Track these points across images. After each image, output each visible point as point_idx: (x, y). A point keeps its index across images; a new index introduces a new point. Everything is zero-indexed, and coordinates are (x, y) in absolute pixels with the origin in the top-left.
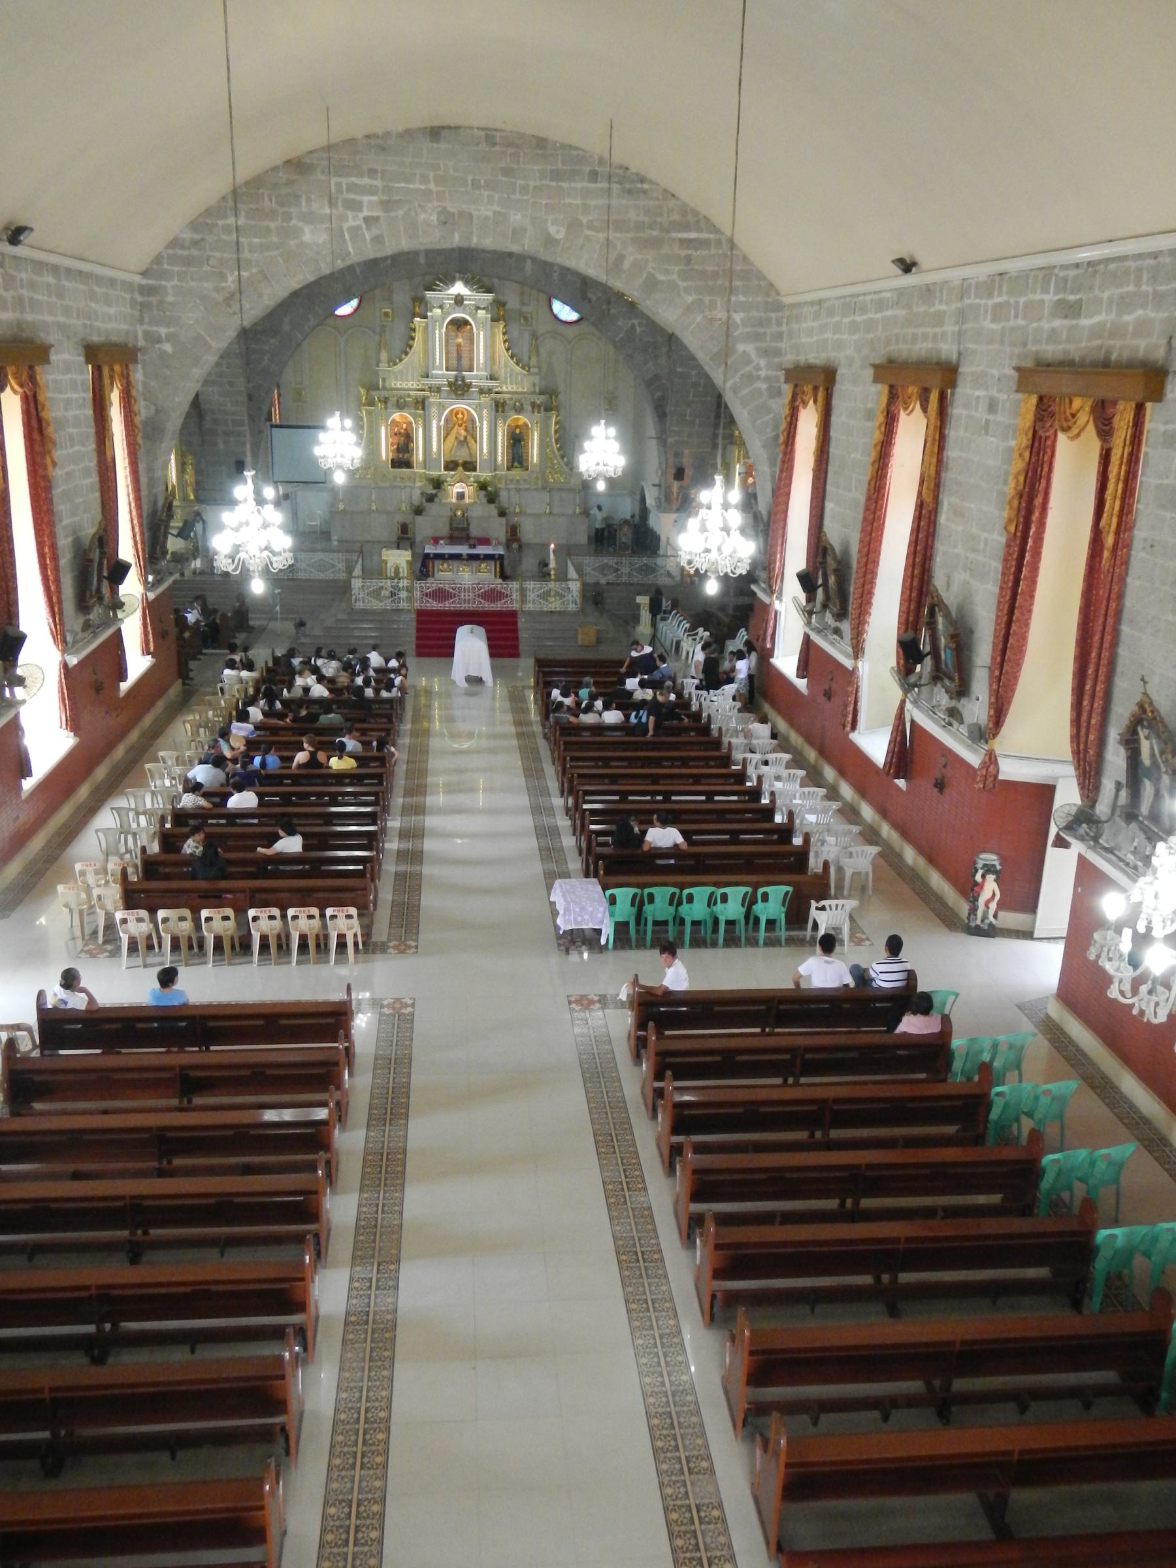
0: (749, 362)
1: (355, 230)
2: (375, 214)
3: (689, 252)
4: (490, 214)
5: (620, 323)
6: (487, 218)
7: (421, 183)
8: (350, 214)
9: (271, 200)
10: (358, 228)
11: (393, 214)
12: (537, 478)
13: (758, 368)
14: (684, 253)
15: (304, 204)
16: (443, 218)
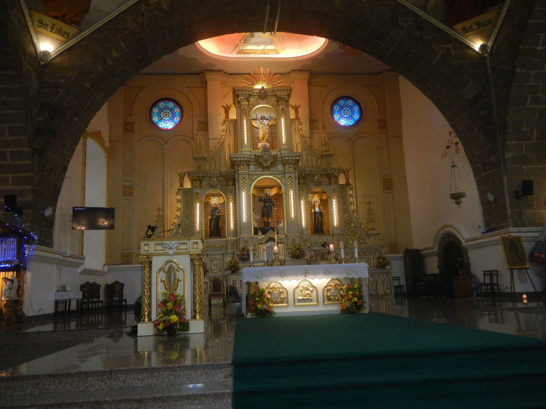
5: (433, 47)
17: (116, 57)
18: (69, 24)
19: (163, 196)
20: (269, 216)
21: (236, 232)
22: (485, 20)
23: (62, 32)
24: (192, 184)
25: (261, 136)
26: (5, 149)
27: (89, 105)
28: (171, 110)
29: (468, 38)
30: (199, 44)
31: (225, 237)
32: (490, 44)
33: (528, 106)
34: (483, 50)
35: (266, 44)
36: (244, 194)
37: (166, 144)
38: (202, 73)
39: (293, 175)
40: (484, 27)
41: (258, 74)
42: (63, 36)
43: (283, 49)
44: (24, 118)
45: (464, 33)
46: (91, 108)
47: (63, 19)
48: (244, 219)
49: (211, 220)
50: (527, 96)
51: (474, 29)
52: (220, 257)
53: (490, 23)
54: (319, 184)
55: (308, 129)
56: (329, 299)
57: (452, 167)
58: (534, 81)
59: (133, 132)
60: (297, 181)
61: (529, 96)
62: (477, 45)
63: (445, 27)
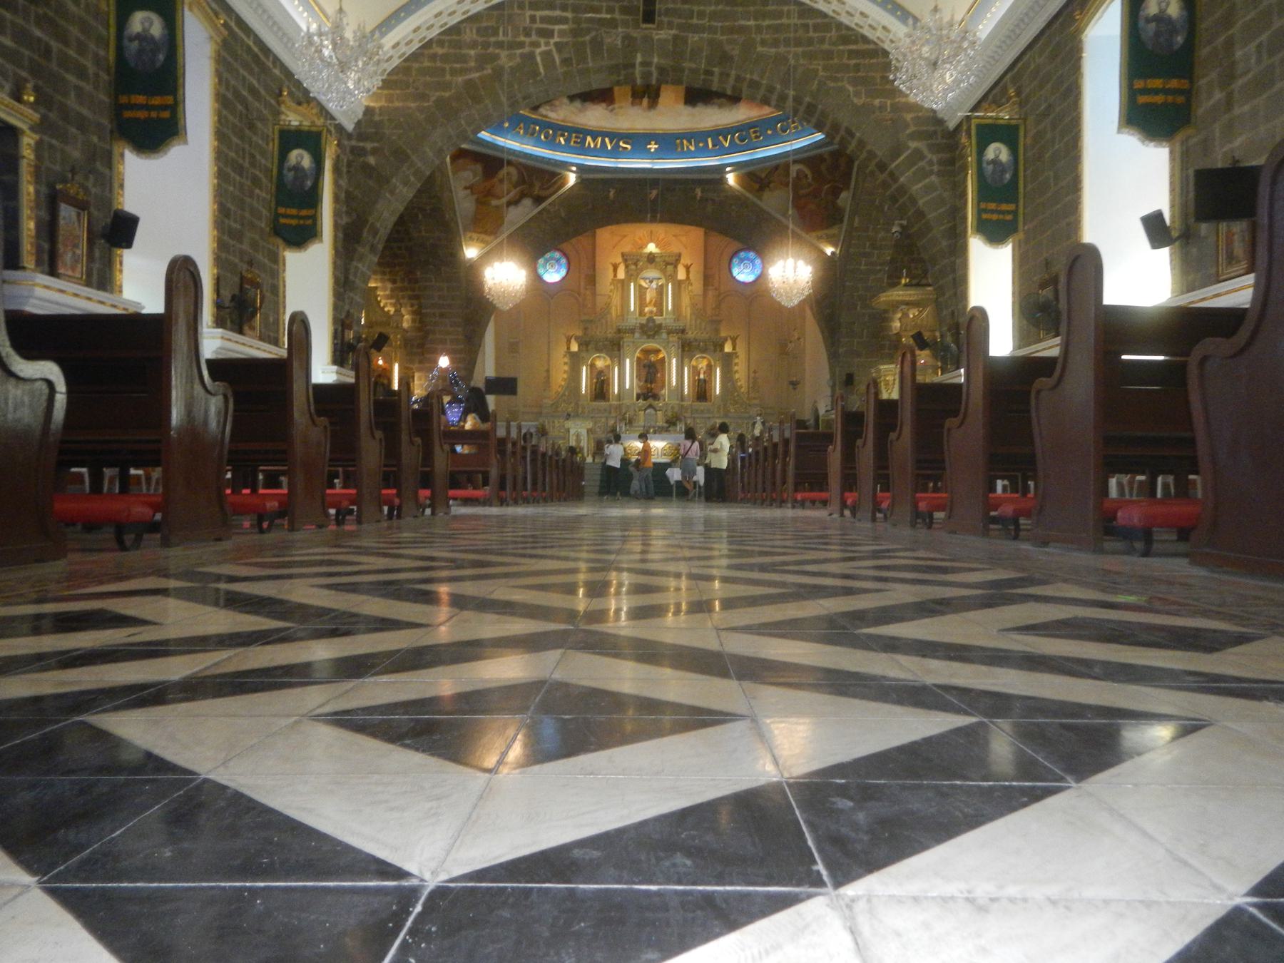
0: (922, 157)
1: (547, 55)
2: (565, 40)
3: (858, 61)
4: (670, 38)
6: (666, 40)
7: (607, 13)
8: (542, 41)
9: (472, 31)
10: (551, 50)
11: (580, 39)
12: (719, 408)
13: (931, 163)
14: (853, 62)
15: (501, 33)
16: (626, 42)
19: (549, 356)
20: (651, 383)
21: (619, 397)
24: (579, 346)
25: (648, 300)
28: (558, 261)
31: (609, 401)
32: (838, 252)
36: (628, 361)
39: (676, 345)
47: (486, 232)
48: (627, 387)
49: (597, 383)
52: (603, 420)
54: (704, 350)
55: (702, 282)
56: (665, 455)
60: (680, 350)
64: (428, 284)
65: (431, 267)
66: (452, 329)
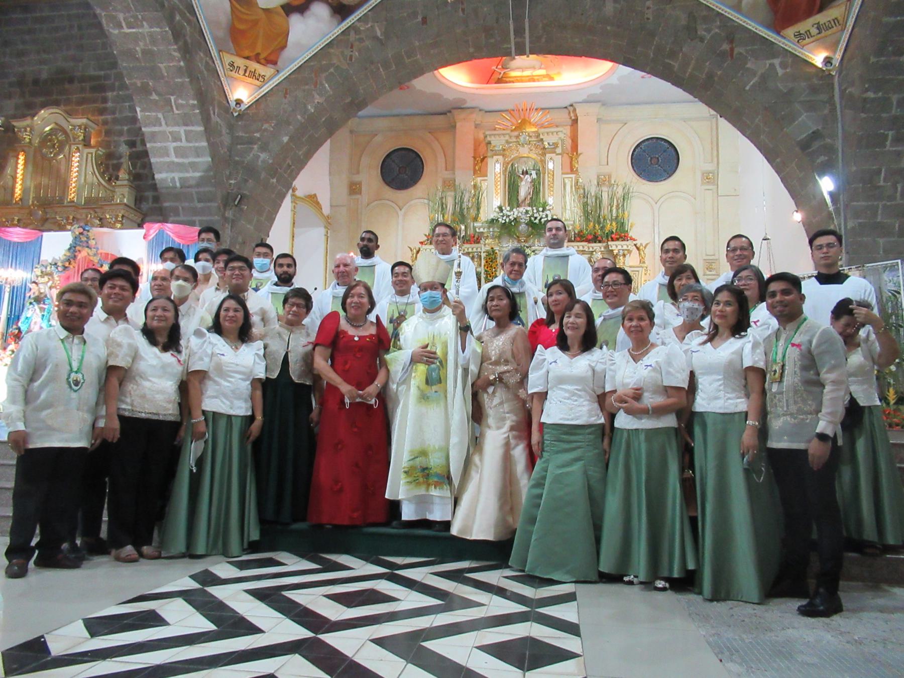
5: (749, 65)
17: (318, 102)
18: (263, 65)
22: (829, 19)
23: (257, 75)
26: (194, 218)
27: (289, 164)
29: (805, 48)
30: (439, 73)
32: (838, 57)
33: (887, 148)
34: (829, 65)
35: (534, 68)
37: (401, 210)
38: (450, 112)
40: (827, 30)
41: (519, 110)
42: (258, 80)
43: (559, 73)
44: (213, 181)
45: (798, 41)
46: (293, 167)
50: (886, 133)
51: (812, 35)
53: (837, 25)
57: (764, 239)
58: (899, 110)
59: (361, 193)
61: (891, 133)
62: (818, 58)
63: (771, 34)
64: (156, 129)
65: (154, 97)
66: (200, 205)
